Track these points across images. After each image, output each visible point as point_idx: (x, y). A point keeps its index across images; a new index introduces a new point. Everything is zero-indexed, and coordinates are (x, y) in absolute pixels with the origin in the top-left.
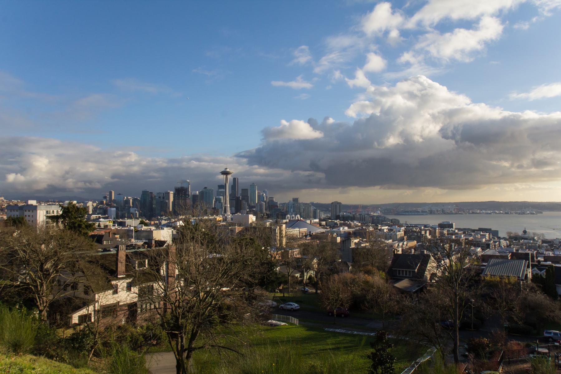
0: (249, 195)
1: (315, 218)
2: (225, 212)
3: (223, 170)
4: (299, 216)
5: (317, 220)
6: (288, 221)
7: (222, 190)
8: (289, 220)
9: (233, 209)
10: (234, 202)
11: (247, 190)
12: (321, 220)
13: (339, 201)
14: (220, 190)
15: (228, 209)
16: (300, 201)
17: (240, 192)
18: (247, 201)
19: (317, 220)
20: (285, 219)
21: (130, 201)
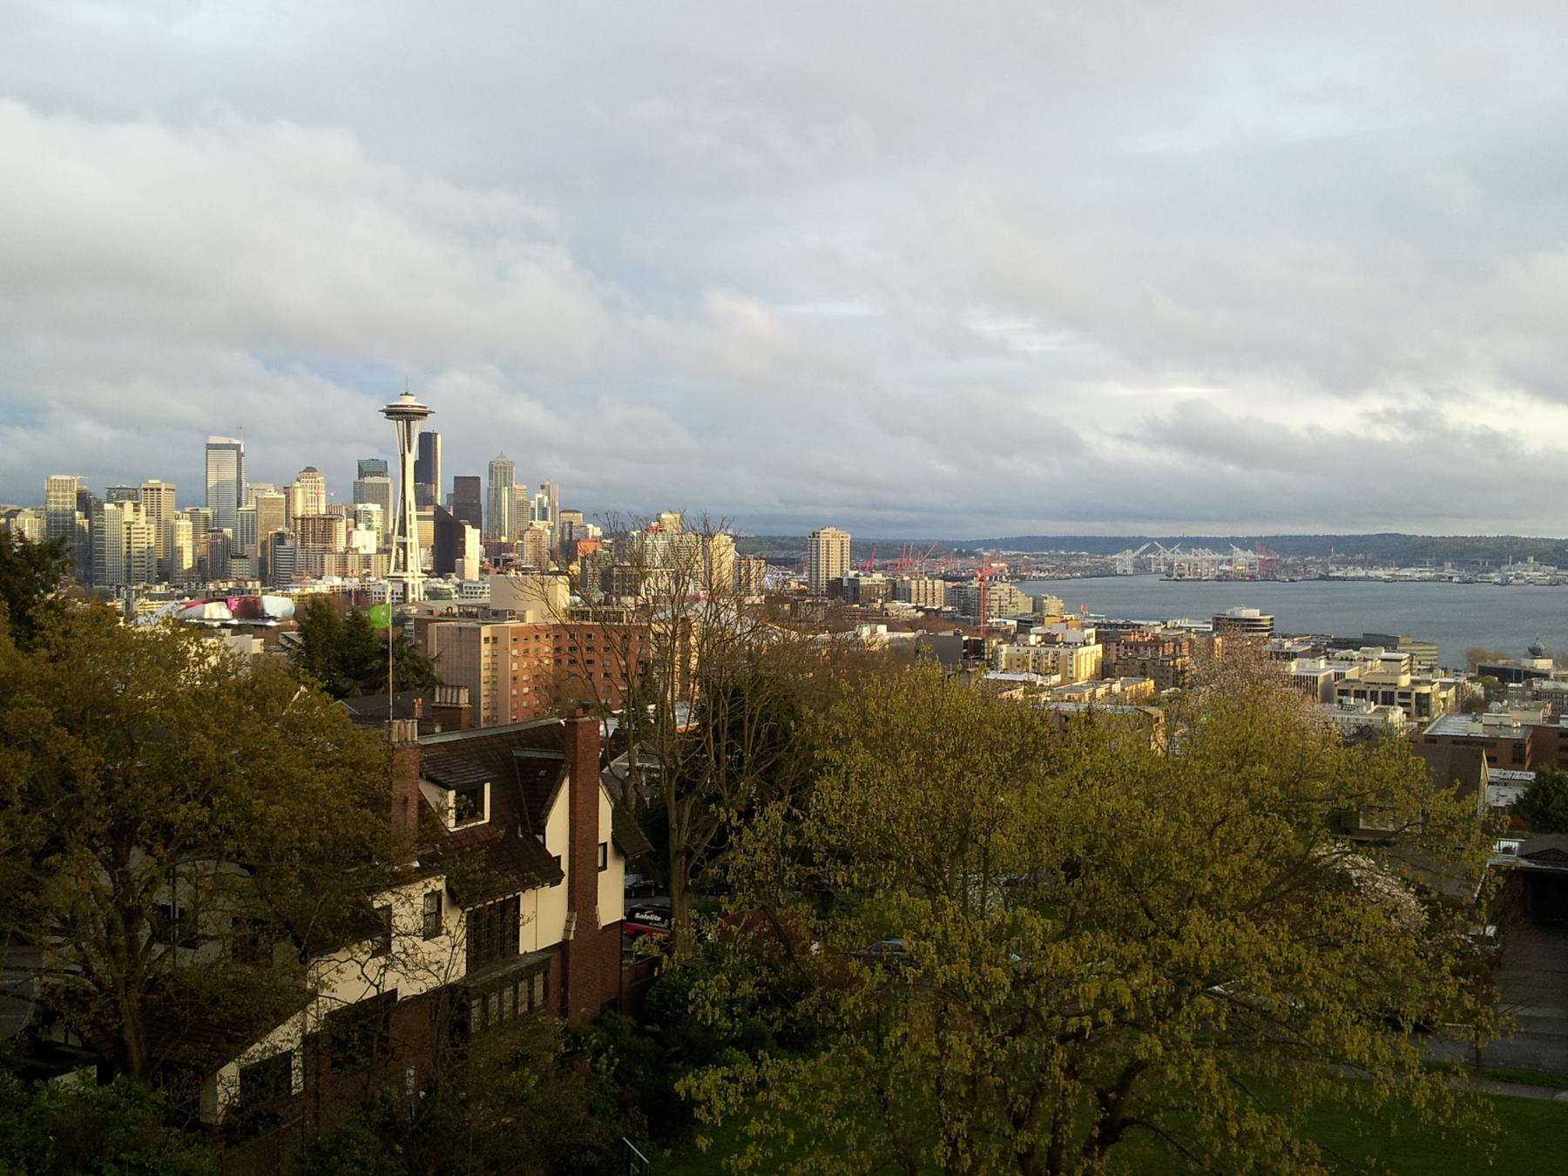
7: (376, 480)
10: (430, 524)
11: (478, 479)
14: (368, 480)
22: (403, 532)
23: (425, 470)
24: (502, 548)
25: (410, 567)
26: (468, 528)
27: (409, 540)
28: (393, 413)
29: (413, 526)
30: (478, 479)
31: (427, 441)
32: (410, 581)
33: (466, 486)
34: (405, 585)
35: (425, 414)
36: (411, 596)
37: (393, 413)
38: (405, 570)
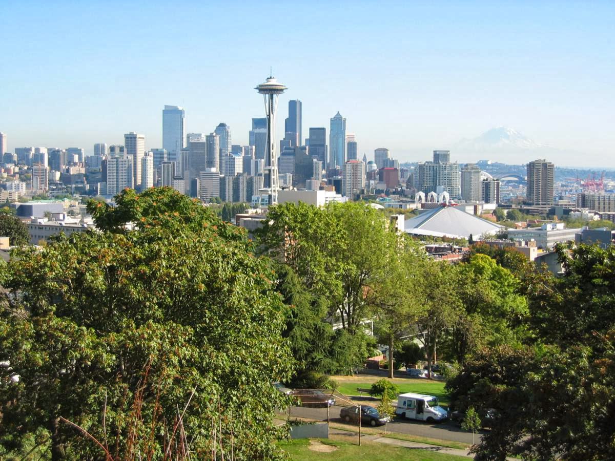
0: (328, 142)
1: (487, 201)
2: (268, 183)
3: (263, 82)
4: (447, 195)
5: (492, 206)
6: (419, 206)
8: (423, 206)
9: (290, 176)
11: (323, 130)
12: (500, 206)
13: (548, 161)
14: (257, 131)
15: (275, 177)
16: (452, 160)
17: (306, 135)
18: (323, 157)
19: (492, 206)
20: (413, 202)
21: (42, 156)
22: (269, 163)
23: (292, 124)
24: (336, 172)
25: (273, 185)
26: (315, 160)
27: (273, 168)
28: (263, 89)
29: (274, 160)
30: (323, 130)
31: (294, 107)
32: (273, 194)
33: (317, 133)
34: (270, 196)
35: (282, 90)
36: (273, 203)
37: (263, 89)
38: (270, 186)
